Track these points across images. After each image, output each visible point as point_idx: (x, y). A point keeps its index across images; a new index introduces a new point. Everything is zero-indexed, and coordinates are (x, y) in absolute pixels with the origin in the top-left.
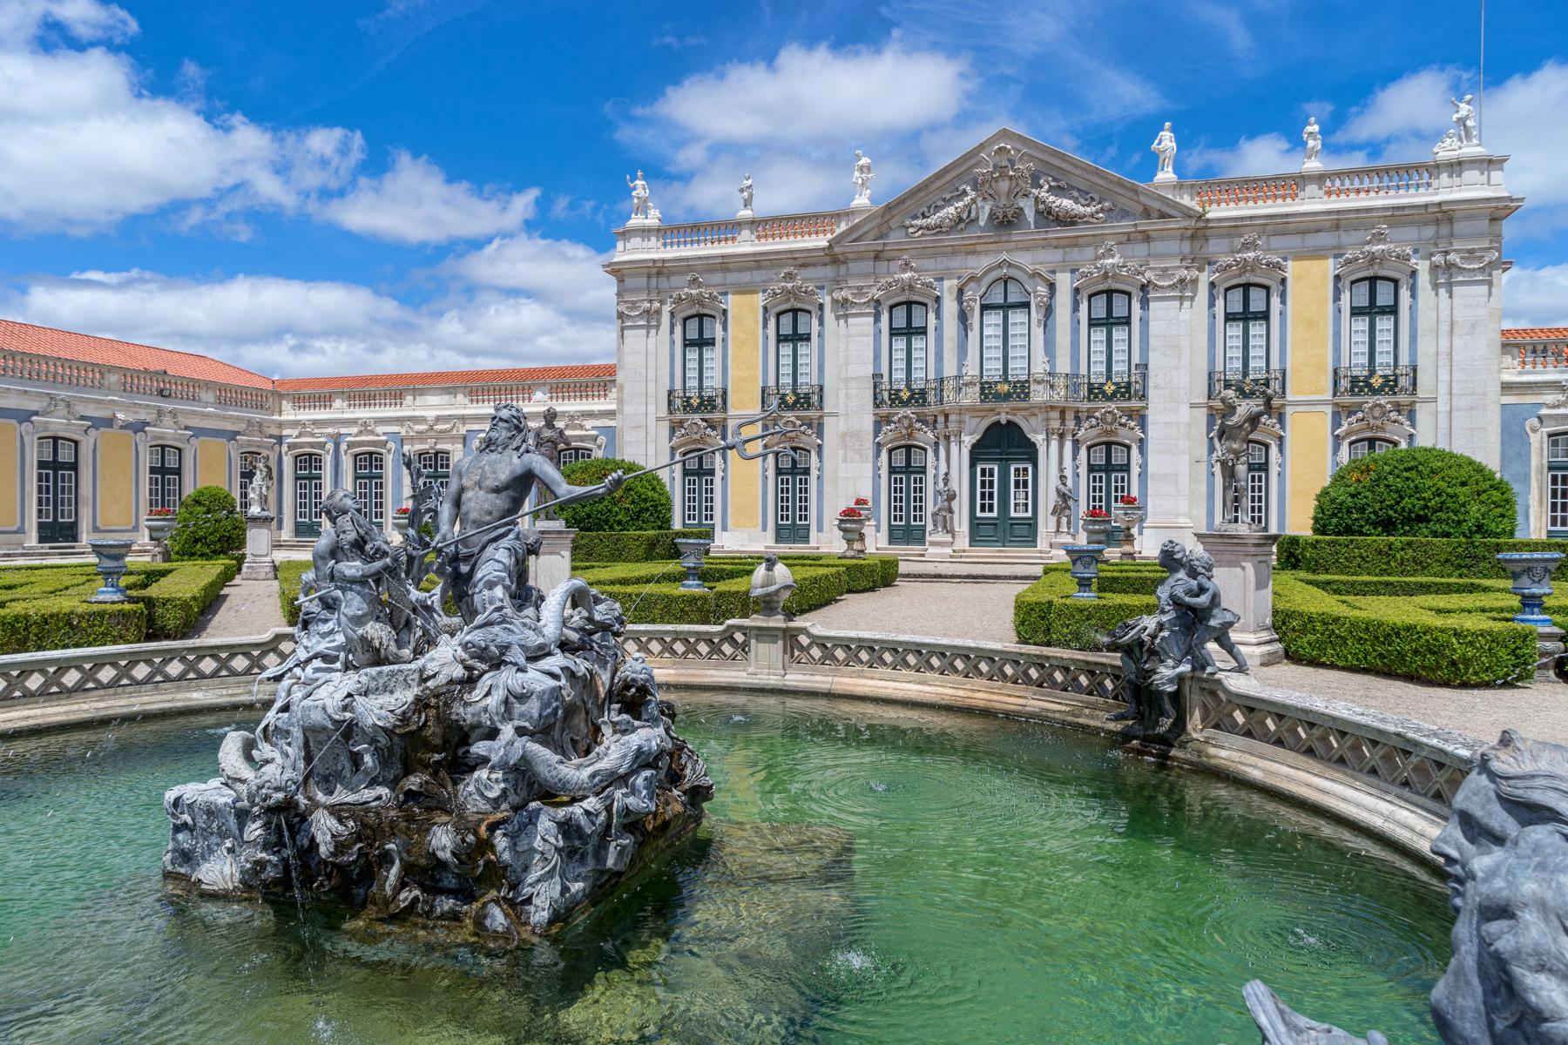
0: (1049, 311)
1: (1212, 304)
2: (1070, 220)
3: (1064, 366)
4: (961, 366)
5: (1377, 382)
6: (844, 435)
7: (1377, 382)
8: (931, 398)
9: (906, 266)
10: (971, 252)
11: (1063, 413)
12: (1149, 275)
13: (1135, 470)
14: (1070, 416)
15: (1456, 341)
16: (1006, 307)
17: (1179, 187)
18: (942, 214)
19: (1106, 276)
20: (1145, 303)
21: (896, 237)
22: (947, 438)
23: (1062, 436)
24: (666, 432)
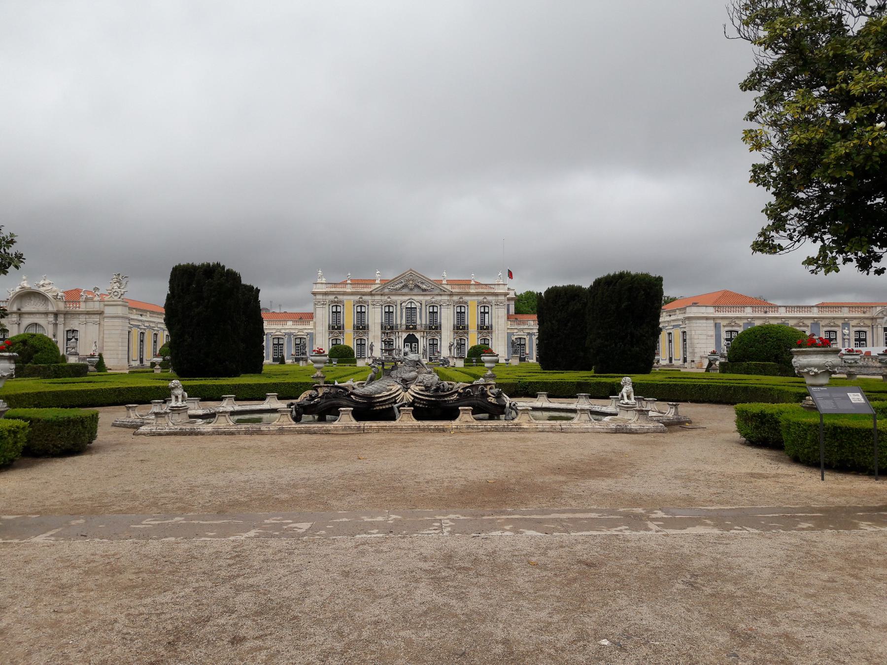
0: (421, 309)
1: (454, 310)
2: (424, 290)
3: (424, 322)
4: (401, 321)
5: (485, 327)
6: (374, 336)
7: (485, 327)
8: (394, 328)
9: (389, 298)
10: (403, 295)
11: (424, 332)
12: (441, 303)
13: (439, 345)
14: (425, 333)
15: (499, 320)
16: (411, 308)
17: (447, 284)
18: (397, 286)
19: (432, 303)
20: (441, 309)
21: (386, 290)
22: (399, 337)
23: (424, 337)
24: (327, 334)
